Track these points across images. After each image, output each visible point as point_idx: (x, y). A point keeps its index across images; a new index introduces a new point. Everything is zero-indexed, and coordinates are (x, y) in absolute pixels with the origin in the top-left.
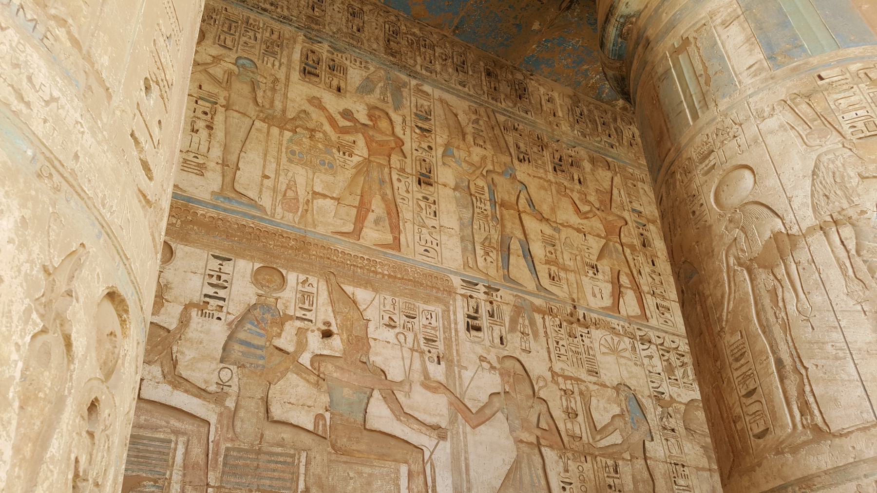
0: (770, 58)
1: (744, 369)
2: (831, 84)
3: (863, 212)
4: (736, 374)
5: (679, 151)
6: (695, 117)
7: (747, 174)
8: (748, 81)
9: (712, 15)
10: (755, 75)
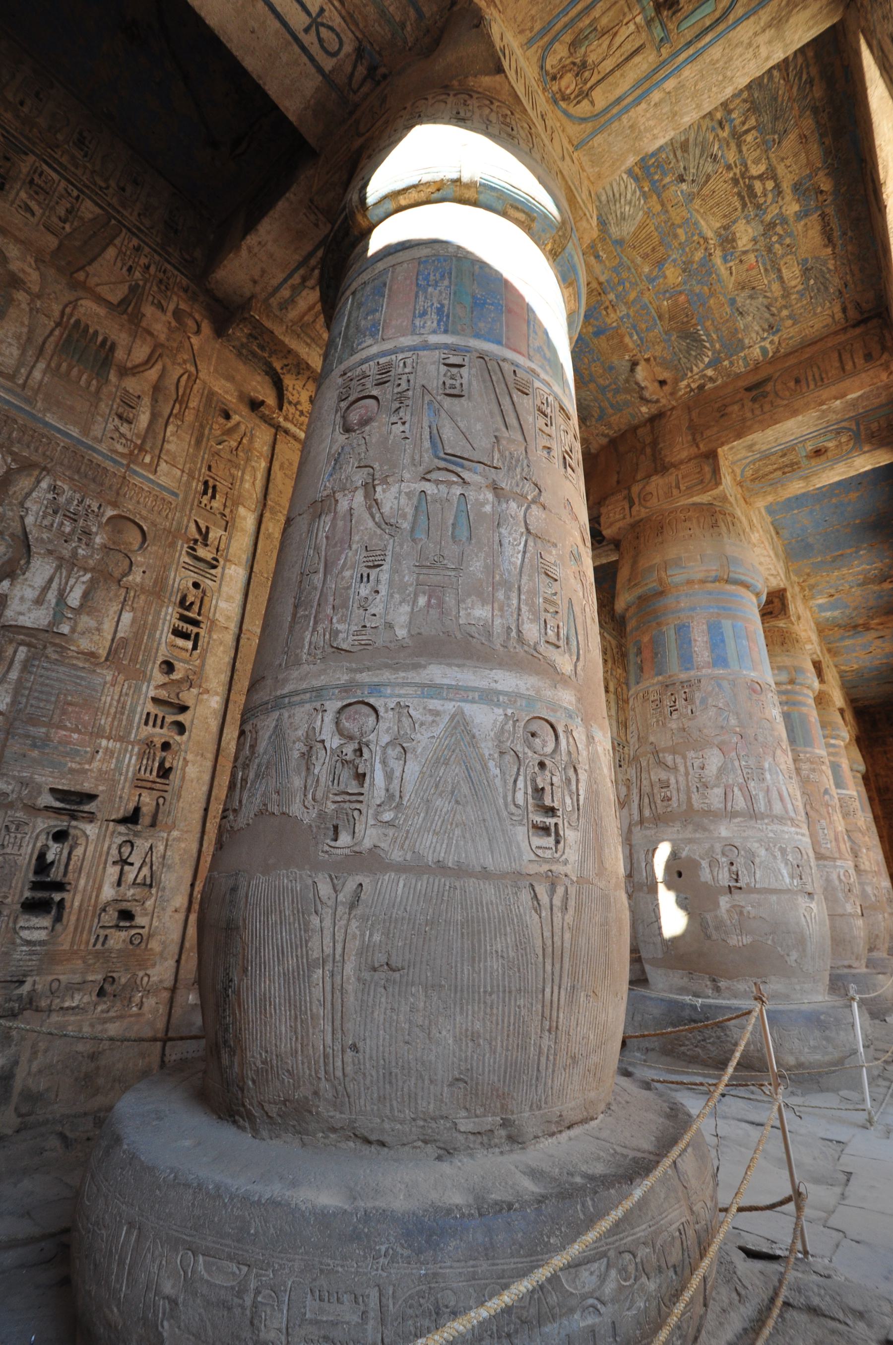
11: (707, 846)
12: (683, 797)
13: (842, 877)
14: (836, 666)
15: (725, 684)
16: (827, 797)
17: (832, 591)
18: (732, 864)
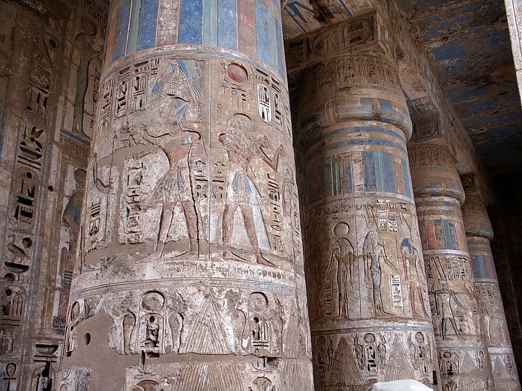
0: (366, 185)
1: (329, 292)
2: (380, 205)
3: (375, 256)
4: (325, 293)
5: (325, 203)
6: (335, 194)
7: (347, 227)
8: (357, 191)
9: (352, 153)
10: (359, 190)
11: (124, 294)
12: (111, 224)
13: (413, 340)
14: (466, 129)
15: (191, 65)
16: (405, 248)
17: (445, 32)
18: (152, 319)
